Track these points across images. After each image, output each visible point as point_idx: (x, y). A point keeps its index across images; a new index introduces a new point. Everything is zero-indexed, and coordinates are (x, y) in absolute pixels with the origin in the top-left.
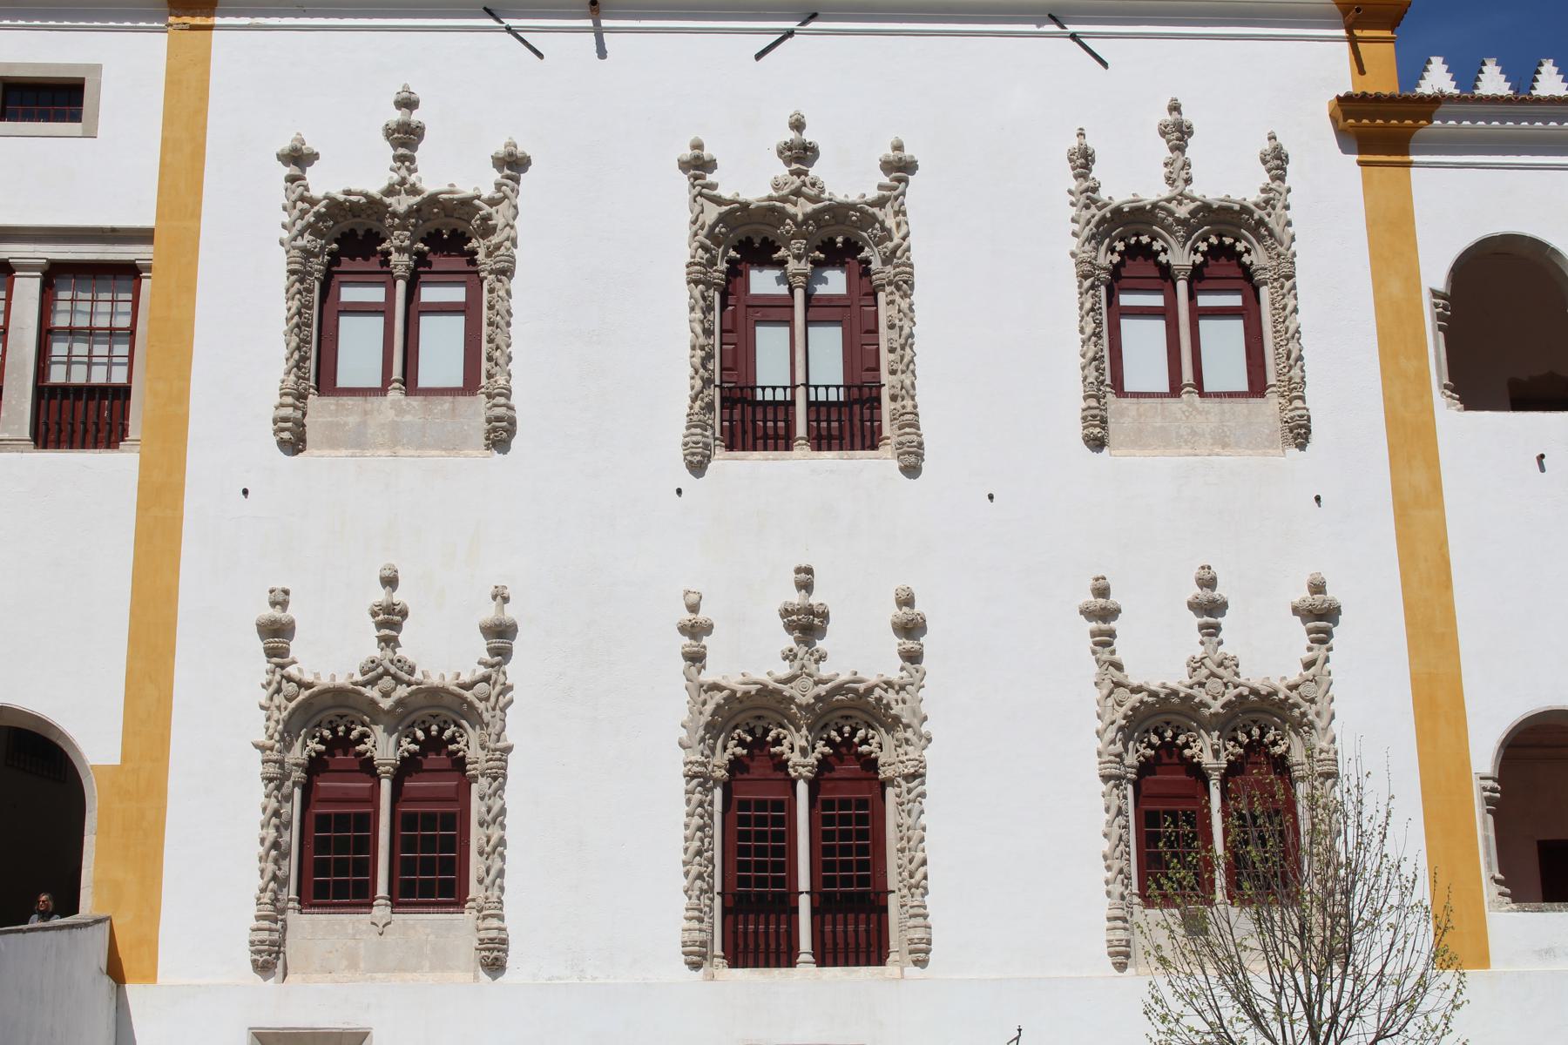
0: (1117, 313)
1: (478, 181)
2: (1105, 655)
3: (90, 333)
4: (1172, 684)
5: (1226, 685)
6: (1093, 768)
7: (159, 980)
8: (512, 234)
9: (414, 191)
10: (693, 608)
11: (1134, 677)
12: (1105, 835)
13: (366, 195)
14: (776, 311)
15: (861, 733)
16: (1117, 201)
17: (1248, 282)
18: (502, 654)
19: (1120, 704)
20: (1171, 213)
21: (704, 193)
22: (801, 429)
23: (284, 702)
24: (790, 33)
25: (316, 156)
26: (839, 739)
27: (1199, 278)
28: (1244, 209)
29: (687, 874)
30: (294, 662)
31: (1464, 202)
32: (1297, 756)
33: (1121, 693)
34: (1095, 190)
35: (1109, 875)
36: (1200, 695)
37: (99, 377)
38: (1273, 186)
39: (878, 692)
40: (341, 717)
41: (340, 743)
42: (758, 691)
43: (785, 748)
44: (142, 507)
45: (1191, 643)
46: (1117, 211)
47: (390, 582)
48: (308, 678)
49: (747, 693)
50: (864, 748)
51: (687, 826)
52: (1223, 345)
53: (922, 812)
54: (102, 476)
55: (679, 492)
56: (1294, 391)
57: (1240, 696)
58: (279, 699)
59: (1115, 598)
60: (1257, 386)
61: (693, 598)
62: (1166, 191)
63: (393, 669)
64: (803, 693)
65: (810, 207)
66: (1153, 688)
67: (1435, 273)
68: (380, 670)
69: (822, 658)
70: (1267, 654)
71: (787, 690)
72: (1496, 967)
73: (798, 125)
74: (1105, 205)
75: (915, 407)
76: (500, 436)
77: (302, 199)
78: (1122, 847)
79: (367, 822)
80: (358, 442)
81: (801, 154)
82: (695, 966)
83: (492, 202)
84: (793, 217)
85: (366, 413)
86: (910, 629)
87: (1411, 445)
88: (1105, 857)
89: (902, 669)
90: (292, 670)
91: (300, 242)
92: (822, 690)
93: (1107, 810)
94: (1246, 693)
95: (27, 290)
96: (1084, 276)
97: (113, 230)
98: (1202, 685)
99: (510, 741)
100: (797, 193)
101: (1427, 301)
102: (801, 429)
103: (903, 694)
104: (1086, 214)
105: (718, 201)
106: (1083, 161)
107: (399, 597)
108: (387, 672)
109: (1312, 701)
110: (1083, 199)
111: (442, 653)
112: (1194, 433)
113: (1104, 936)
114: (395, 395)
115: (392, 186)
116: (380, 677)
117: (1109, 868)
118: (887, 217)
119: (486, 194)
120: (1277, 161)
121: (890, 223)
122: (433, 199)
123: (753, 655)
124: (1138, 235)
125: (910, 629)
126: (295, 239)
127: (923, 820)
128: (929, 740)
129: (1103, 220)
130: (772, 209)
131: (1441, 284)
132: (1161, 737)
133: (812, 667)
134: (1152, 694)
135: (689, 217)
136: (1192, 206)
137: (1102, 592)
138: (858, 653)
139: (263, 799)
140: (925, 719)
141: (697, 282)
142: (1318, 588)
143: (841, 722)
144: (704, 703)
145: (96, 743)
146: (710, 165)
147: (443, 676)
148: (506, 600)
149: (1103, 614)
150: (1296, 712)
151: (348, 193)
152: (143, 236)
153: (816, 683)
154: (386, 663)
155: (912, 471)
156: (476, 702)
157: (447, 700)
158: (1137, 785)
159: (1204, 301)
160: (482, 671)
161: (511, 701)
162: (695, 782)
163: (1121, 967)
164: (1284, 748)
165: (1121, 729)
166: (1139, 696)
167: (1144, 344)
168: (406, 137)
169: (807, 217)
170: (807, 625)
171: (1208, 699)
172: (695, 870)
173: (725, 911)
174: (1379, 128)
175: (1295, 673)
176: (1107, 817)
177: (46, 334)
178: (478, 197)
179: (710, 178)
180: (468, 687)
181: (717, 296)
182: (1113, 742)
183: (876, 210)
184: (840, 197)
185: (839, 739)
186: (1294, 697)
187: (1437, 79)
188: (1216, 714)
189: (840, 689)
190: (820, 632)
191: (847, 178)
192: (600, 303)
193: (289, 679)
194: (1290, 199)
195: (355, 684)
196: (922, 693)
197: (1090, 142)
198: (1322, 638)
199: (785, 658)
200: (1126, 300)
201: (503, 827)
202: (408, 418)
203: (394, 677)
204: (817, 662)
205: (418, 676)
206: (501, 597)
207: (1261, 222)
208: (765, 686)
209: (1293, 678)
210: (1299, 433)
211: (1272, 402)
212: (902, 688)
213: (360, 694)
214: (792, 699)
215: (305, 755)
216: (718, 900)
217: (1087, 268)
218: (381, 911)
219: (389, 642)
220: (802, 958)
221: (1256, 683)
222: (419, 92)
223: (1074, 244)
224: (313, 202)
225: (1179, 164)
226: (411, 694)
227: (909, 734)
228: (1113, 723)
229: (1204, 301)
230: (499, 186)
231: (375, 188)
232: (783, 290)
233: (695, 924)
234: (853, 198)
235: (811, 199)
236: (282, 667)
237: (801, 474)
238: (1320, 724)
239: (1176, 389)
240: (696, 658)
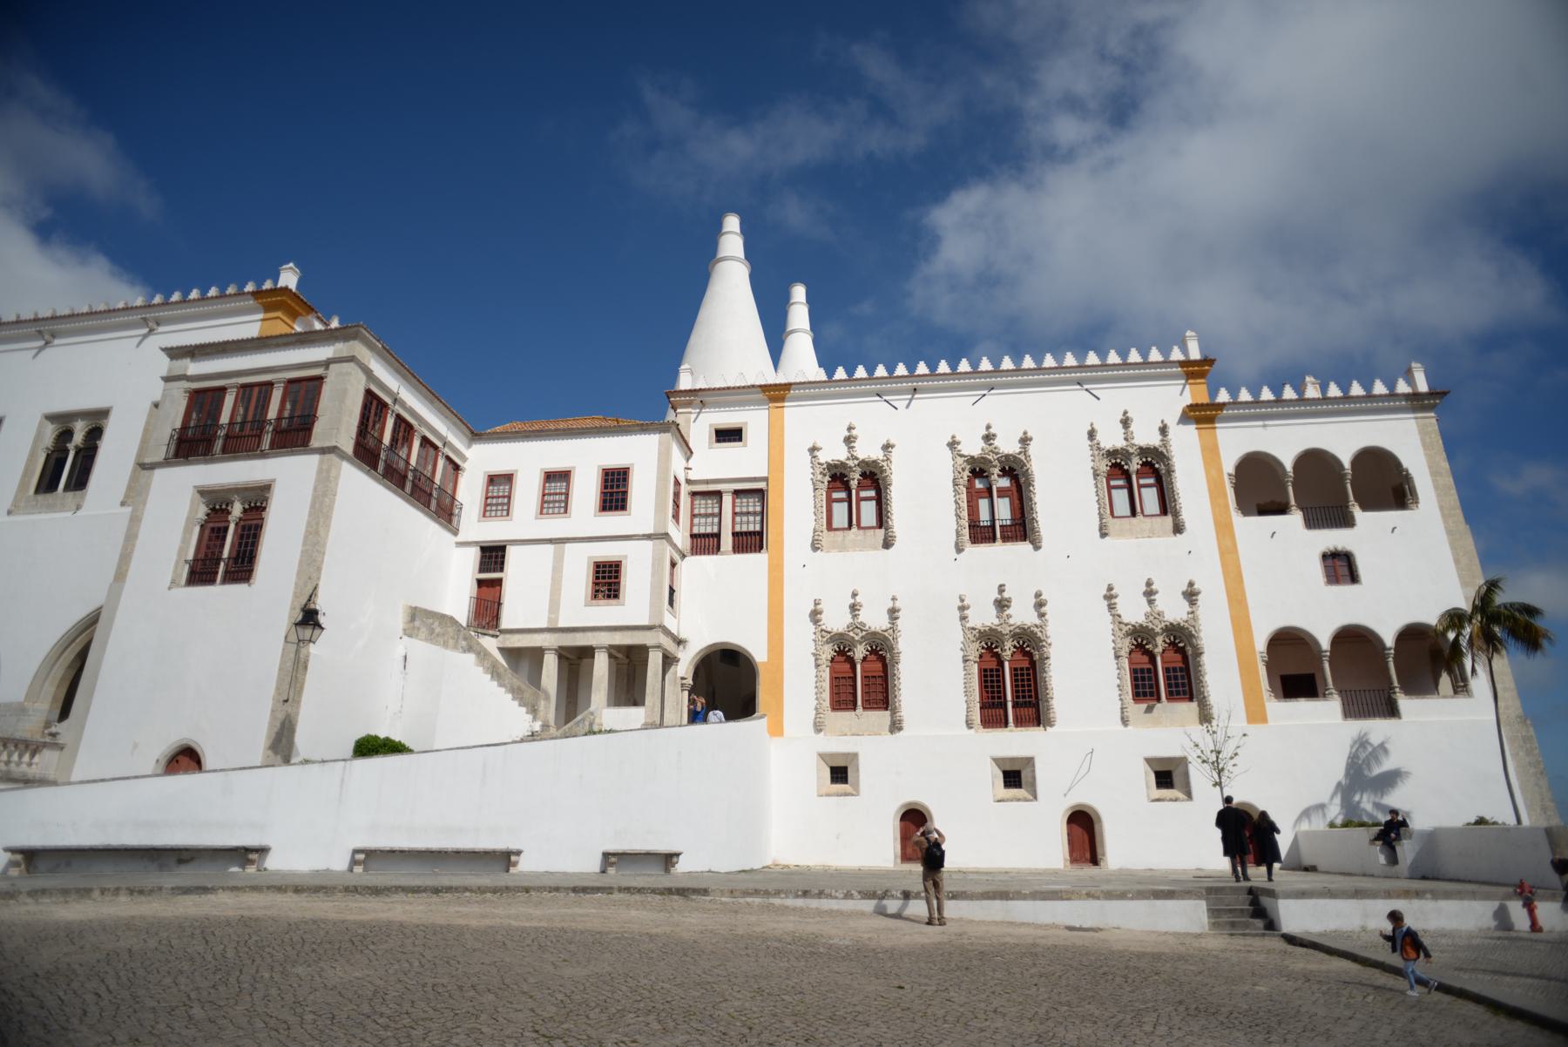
1: (877, 454)
3: (748, 513)
11: (1125, 619)
27: (1140, 474)
31: (1235, 441)
37: (751, 528)
54: (755, 562)
56: (1176, 514)
60: (1164, 511)
67: (1229, 467)
69: (1009, 616)
70: (1174, 610)
72: (1271, 723)
73: (988, 427)
76: (887, 544)
80: (842, 548)
81: (988, 438)
86: (1040, 605)
87: (1224, 530)
101: (1226, 478)
106: (1092, 434)
111: (875, 620)
114: (855, 529)
118: (1022, 457)
120: (1163, 430)
123: (983, 616)
125: (1040, 605)
131: (1232, 471)
137: (1110, 588)
138: (1022, 615)
142: (1191, 584)
145: (759, 654)
149: (1110, 597)
152: (766, 479)
155: (1037, 548)
159: (1142, 482)
167: (1121, 497)
168: (849, 440)
170: (1002, 604)
174: (1202, 415)
187: (1223, 396)
191: (1008, 445)
198: (1192, 603)
200: (1113, 483)
206: (894, 599)
209: (1185, 617)
210: (1178, 529)
219: (854, 617)
222: (855, 424)
229: (1142, 482)
239: (1134, 513)
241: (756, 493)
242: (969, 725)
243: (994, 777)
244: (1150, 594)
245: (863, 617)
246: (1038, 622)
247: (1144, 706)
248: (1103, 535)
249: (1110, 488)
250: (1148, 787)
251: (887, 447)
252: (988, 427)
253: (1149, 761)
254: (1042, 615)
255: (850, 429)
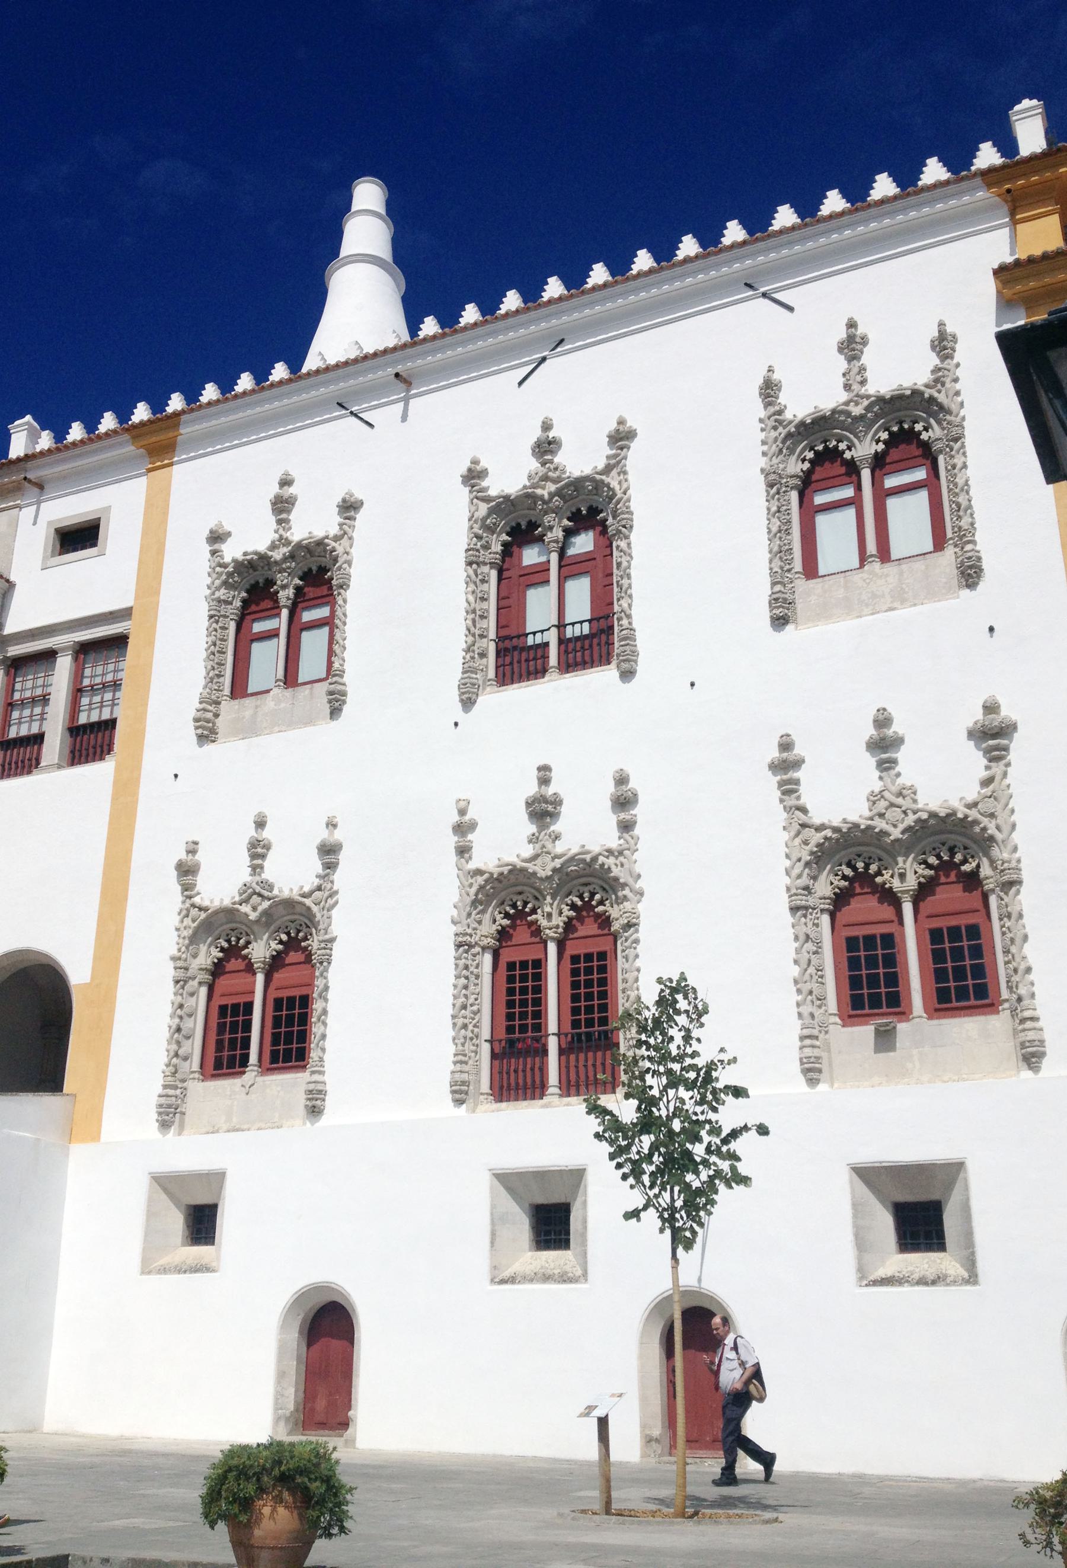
0: (809, 513)
2: (791, 801)
4: (854, 818)
5: (905, 812)
6: (783, 902)
7: (102, 1140)
8: (349, 557)
9: (288, 542)
10: (462, 812)
11: (817, 817)
12: (796, 962)
13: (256, 553)
14: (538, 576)
15: (597, 897)
16: (800, 416)
17: (928, 455)
18: (330, 867)
19: (806, 843)
20: (848, 414)
21: (479, 495)
22: (553, 660)
23: (190, 923)
24: (544, 359)
25: (229, 534)
26: (580, 903)
28: (916, 393)
29: (454, 1024)
30: (199, 894)
32: (986, 871)
33: (808, 833)
34: (780, 412)
35: (800, 998)
36: (880, 825)
38: (944, 365)
39: (601, 859)
40: (233, 930)
41: (232, 951)
42: (510, 871)
43: (538, 916)
44: (115, 798)
45: (870, 779)
46: (802, 424)
47: (260, 824)
48: (206, 903)
49: (502, 874)
50: (601, 908)
51: (455, 986)
52: (908, 517)
53: (637, 956)
55: (456, 724)
56: (965, 537)
57: (919, 821)
58: (188, 921)
59: (798, 751)
61: (462, 804)
62: (844, 396)
63: (258, 889)
64: (543, 869)
65: (552, 487)
66: (835, 824)
68: (250, 891)
69: (557, 837)
71: (531, 867)
73: (547, 426)
74: (791, 422)
75: (630, 623)
76: (336, 706)
77: (220, 565)
78: (811, 970)
79: (249, 1007)
81: (546, 448)
82: (459, 1102)
83: (337, 538)
84: (541, 498)
85: (257, 707)
86: (623, 802)
88: (796, 982)
89: (620, 838)
90: (197, 900)
91: (217, 594)
92: (558, 863)
93: (796, 938)
94: (925, 816)
95: (64, 664)
96: (771, 485)
97: (111, 613)
98: (881, 815)
99: (335, 934)
100: (545, 478)
102: (553, 660)
103: (621, 859)
104: (774, 434)
105: (487, 500)
106: (769, 390)
107: (267, 834)
108: (255, 893)
109: (992, 816)
110: (771, 423)
111: (291, 873)
112: (874, 596)
113: (796, 1055)
115: (273, 542)
116: (250, 897)
117: (799, 991)
119: (332, 534)
120: (943, 344)
121: (614, 484)
122: (299, 546)
124: (825, 442)
125: (623, 802)
126: (213, 594)
127: (638, 963)
128: (642, 894)
129: (789, 435)
130: (528, 496)
132: (854, 868)
133: (549, 846)
134: (836, 830)
135: (468, 514)
136: (866, 403)
137: (786, 745)
139: (172, 997)
140: (639, 876)
141: (470, 564)
143: (582, 889)
144: (471, 886)
146: (483, 474)
147: (291, 890)
148: (335, 826)
149: (786, 766)
150: (977, 829)
151: (245, 554)
152: (125, 614)
153: (553, 859)
154: (254, 885)
156: (313, 906)
157: (298, 909)
158: (833, 916)
160: (317, 882)
161: (337, 903)
162: (461, 949)
163: (812, 1082)
164: (974, 864)
165: (807, 864)
166: (824, 833)
167: (837, 533)
168: (282, 506)
169: (552, 495)
170: (543, 811)
171: (889, 828)
172: (460, 1022)
173: (494, 1056)
175: (973, 793)
176: (797, 945)
177: (77, 691)
178: (327, 537)
179: (484, 484)
180: (304, 896)
181: (494, 574)
182: (799, 876)
183: (604, 477)
184: (577, 474)
185: (580, 903)
186: (973, 814)
188: (897, 840)
189: (572, 859)
190: (554, 816)
191: (580, 459)
192: (409, 596)
193: (193, 906)
194: (959, 372)
195: (234, 903)
196: (636, 856)
197: (776, 376)
199: (530, 842)
201: (326, 1000)
202: (283, 705)
203: (260, 895)
204: (554, 841)
205: (276, 892)
206: (332, 825)
207: (932, 400)
208: (515, 866)
209: (972, 796)
210: (970, 574)
211: (950, 551)
212: (621, 853)
213: (238, 910)
214: (535, 874)
215: (209, 962)
216: (486, 1048)
217: (772, 477)
218: (251, 1074)
219: (256, 869)
220: (551, 1090)
221: (935, 806)
222: (294, 474)
223: (763, 462)
224: (224, 566)
225: (855, 370)
226: (270, 907)
227: (627, 892)
228: (799, 860)
230: (341, 525)
231: (262, 547)
232: (543, 559)
233: (458, 1067)
234: (587, 471)
235: (555, 481)
236: (190, 897)
237: (556, 693)
238: (999, 836)
240: (463, 851)
241: (105, 645)
242: (460, 1094)
243: (497, 1222)
244: (884, 746)
245: (271, 870)
246: (614, 843)
247: (866, 1032)
248: (780, 622)
249: (809, 513)
250: (861, 1244)
251: (349, 508)
252: (547, 426)
253: (869, 1176)
254: (626, 827)
255: (286, 482)
